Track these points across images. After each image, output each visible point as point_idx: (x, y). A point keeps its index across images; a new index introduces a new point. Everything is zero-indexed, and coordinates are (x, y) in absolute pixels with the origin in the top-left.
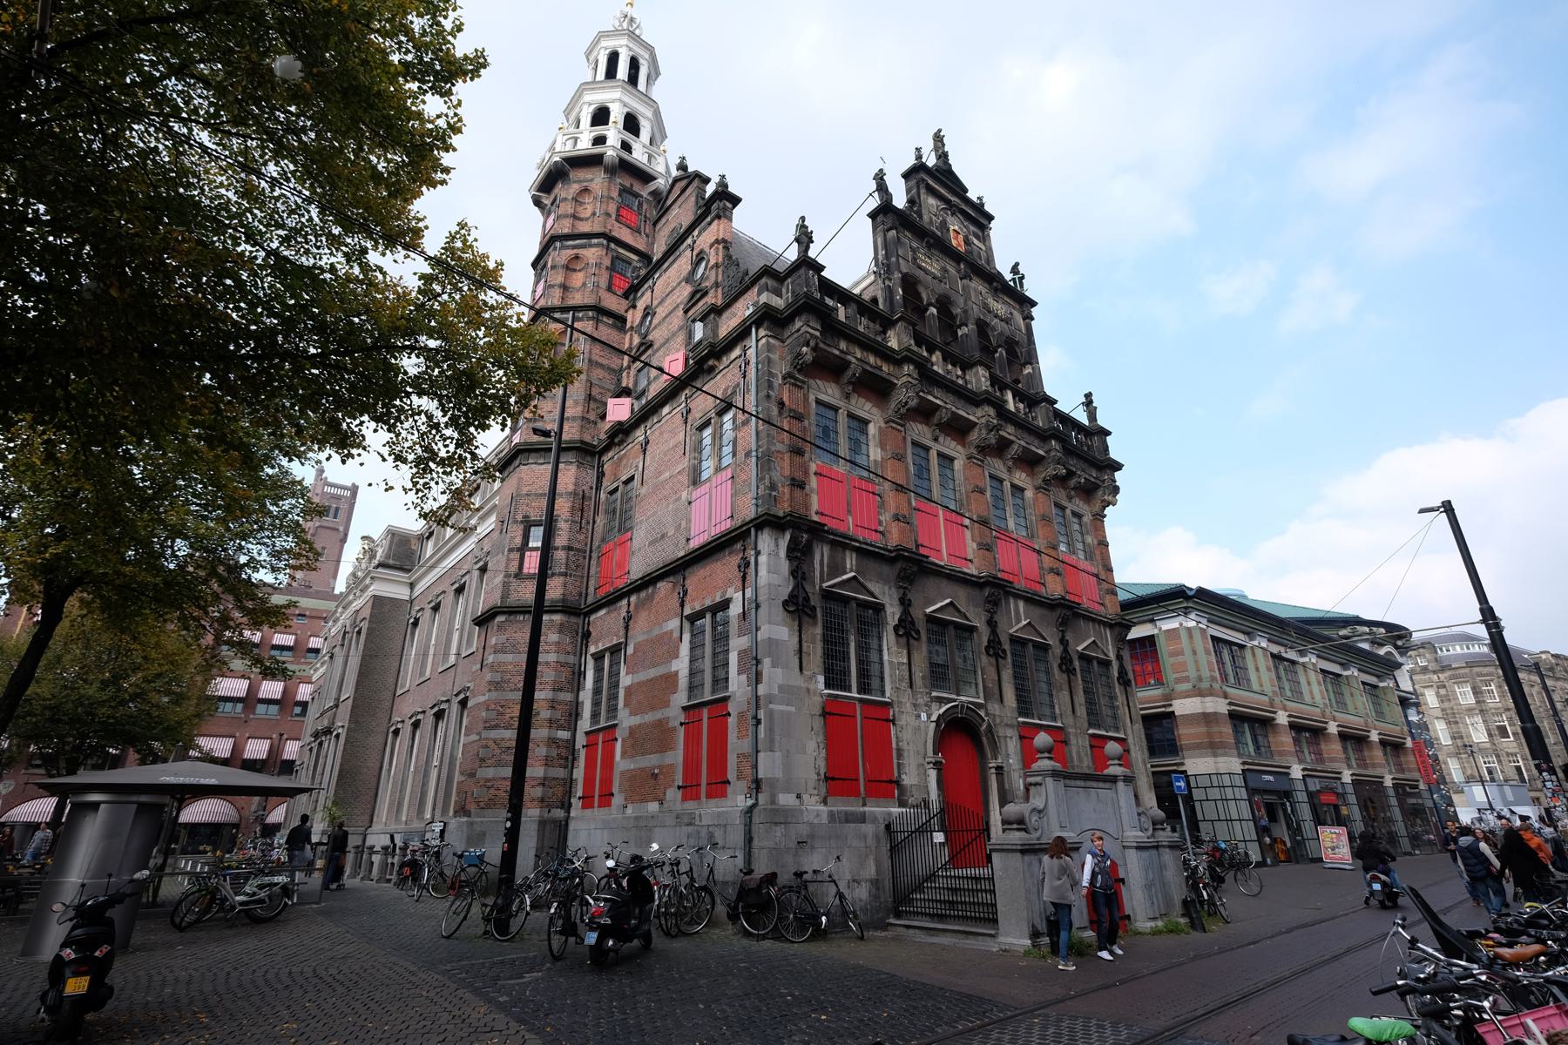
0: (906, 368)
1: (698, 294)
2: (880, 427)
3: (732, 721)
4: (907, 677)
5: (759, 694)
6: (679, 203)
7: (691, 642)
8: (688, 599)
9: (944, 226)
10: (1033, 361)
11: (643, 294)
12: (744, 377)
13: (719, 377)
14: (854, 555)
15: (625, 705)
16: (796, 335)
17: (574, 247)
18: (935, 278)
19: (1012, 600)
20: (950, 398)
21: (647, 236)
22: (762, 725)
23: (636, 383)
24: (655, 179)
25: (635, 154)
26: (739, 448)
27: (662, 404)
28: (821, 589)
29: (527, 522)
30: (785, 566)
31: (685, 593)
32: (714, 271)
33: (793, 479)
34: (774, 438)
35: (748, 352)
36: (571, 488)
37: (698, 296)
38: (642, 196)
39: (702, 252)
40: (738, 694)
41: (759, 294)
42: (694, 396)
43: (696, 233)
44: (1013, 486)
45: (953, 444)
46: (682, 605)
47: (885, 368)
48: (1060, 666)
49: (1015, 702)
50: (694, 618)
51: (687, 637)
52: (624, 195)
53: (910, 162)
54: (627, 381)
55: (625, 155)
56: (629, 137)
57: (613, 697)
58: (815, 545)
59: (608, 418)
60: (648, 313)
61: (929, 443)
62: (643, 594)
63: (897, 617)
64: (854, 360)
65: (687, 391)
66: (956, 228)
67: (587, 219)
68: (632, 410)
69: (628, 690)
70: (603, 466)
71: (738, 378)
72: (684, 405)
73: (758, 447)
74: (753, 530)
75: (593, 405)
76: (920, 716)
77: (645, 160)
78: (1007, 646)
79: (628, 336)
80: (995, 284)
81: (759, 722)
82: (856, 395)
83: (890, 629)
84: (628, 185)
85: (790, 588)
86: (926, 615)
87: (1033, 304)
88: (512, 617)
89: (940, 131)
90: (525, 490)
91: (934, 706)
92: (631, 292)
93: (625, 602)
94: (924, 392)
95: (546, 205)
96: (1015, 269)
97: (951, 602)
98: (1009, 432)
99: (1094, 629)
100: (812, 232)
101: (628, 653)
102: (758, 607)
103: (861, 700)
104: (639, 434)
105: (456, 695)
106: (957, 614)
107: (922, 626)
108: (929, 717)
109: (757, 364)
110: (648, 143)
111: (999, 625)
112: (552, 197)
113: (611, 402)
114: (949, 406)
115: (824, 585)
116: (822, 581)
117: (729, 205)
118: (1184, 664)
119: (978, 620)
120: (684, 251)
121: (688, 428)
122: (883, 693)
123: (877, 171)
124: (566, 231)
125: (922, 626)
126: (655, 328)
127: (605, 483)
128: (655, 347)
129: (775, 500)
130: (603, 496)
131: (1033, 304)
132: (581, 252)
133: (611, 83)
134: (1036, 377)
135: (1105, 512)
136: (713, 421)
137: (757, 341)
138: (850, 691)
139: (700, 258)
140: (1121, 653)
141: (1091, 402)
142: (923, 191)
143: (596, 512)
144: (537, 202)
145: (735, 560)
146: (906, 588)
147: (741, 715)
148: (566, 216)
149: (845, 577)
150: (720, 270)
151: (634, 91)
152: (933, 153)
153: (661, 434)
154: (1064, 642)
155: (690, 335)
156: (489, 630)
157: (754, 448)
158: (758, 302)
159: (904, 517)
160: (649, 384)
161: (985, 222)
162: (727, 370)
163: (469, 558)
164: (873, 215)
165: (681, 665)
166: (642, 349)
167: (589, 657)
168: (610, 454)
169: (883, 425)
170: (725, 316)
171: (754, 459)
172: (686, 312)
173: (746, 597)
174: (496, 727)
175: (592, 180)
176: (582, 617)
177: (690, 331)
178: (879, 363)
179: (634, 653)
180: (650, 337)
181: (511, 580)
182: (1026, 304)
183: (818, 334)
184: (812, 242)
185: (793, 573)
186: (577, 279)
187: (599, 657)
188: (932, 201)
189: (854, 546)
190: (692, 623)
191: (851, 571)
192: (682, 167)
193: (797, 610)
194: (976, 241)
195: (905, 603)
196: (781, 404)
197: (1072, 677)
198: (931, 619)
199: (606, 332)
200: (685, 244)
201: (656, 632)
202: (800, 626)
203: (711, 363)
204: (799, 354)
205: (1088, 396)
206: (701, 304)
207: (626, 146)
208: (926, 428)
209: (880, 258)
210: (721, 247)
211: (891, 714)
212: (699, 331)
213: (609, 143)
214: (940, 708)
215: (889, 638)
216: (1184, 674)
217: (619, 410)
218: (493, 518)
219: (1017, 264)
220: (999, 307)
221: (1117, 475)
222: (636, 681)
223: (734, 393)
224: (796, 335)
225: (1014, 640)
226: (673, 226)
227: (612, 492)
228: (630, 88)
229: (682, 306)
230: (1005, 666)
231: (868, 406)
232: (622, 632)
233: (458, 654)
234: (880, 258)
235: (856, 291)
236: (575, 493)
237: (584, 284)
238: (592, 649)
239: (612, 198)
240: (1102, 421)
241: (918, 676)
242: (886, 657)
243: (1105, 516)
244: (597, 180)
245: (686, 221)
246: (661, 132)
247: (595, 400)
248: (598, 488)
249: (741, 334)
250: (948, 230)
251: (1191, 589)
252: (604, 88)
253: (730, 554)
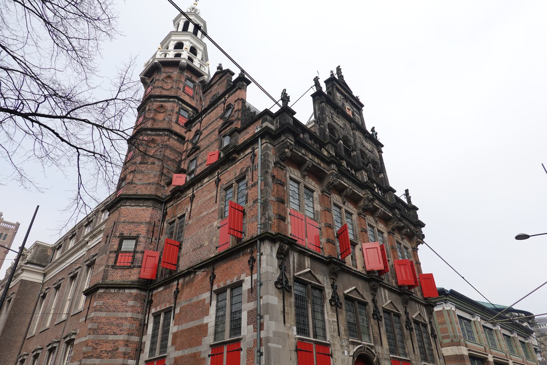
0: (332, 166)
1: (228, 123)
2: (319, 195)
3: (243, 354)
4: (337, 329)
5: (261, 337)
6: (218, 83)
7: (217, 306)
8: (216, 281)
9: (343, 104)
10: (384, 171)
11: (195, 125)
12: (253, 163)
13: (238, 163)
14: (309, 260)
15: (173, 344)
16: (282, 143)
17: (160, 101)
18: (341, 127)
19: (382, 289)
20: (350, 183)
21: (197, 101)
22: (264, 356)
23: (188, 167)
24: (203, 76)
25: (194, 63)
26: (249, 198)
27: (204, 178)
28: (294, 277)
29: (122, 237)
30: (276, 262)
31: (214, 277)
32: (237, 113)
33: (280, 216)
34: (270, 194)
35: (256, 151)
36: (148, 220)
37: (227, 124)
38: (196, 83)
39: (230, 104)
40: (247, 337)
41: (262, 123)
42: (223, 173)
43: (227, 96)
44: (379, 231)
45: (352, 207)
46: (212, 285)
47: (322, 165)
48: (406, 326)
49: (388, 346)
50: (220, 292)
51: (214, 303)
52: (187, 81)
53: (328, 76)
54: (184, 166)
55: (190, 63)
56: (192, 56)
57: (165, 339)
58: (290, 252)
59: (173, 184)
60: (198, 134)
61: (341, 205)
62: (187, 279)
63: (331, 295)
64: (308, 159)
65: (219, 170)
66: (349, 107)
67: (168, 90)
68: (186, 180)
69: (175, 335)
70: (166, 209)
71: (249, 163)
72: (216, 177)
73: (262, 197)
74: (258, 242)
75: (163, 177)
76: (344, 353)
77: (199, 66)
78: (382, 314)
79: (186, 144)
80: (366, 134)
81: (261, 354)
82: (308, 177)
83: (327, 301)
84: (190, 77)
85: (278, 275)
86: (344, 294)
87: (382, 146)
88: (108, 291)
89: (339, 66)
90: (122, 219)
91: (351, 346)
92: (188, 125)
93: (176, 283)
94: (340, 179)
95: (147, 83)
96: (373, 130)
97: (356, 289)
98: (377, 203)
99: (419, 307)
100: (289, 96)
101: (175, 313)
102: (261, 285)
103: (315, 342)
104: (189, 193)
105: (65, 338)
106: (358, 295)
107: (342, 300)
108: (349, 353)
109: (261, 156)
110: (200, 59)
111: (378, 302)
112: (151, 79)
113: (175, 175)
114: (351, 187)
115: (296, 274)
116: (294, 272)
117: (245, 84)
118: (446, 329)
119: (368, 299)
120: (220, 104)
121: (219, 189)
122: (325, 338)
123: (315, 77)
124: (157, 94)
125: (342, 300)
126: (202, 140)
127: (167, 218)
128: (201, 149)
129: (271, 226)
130: (165, 225)
131: (382, 146)
132: (164, 104)
133: (185, 33)
134: (385, 179)
135: (418, 247)
136: (234, 185)
137: (261, 145)
138: (309, 336)
139: (229, 107)
140: (431, 320)
141: (408, 194)
142: (335, 89)
143: (161, 233)
144: (143, 81)
145: (246, 258)
146: (334, 279)
147: (249, 350)
148: (158, 87)
149: (305, 271)
150: (240, 113)
151: (195, 37)
153: (203, 192)
154: (406, 313)
155: (221, 143)
156: (93, 298)
157: (259, 198)
158: (262, 126)
159: (332, 241)
160: (197, 167)
161: (360, 107)
162: (243, 159)
163: (81, 259)
164: (313, 96)
165: (210, 320)
166: (194, 150)
167: (151, 315)
168: (171, 203)
169: (320, 193)
170: (242, 134)
171: (259, 204)
172: (220, 132)
173: (253, 279)
174: (91, 357)
175: (172, 72)
176: (148, 291)
177: (222, 141)
178: (319, 162)
179: (180, 312)
180: (198, 145)
181: (110, 268)
182: (379, 145)
183: (293, 143)
184: (289, 101)
185: (280, 266)
186: (160, 117)
187: (157, 316)
188: (338, 94)
189: (309, 254)
190: (218, 295)
191: (308, 268)
192: (220, 67)
193: (282, 288)
194: (356, 115)
195: (333, 287)
196: (273, 177)
197: (412, 333)
199: (173, 142)
200: (220, 101)
201: (195, 300)
202: (283, 297)
203: (234, 156)
204: (284, 152)
205: (407, 191)
206: (228, 128)
207: (190, 59)
208: (339, 198)
209: (317, 115)
210: (241, 102)
211: (330, 351)
212: (226, 142)
213: (182, 57)
214: (354, 348)
215: (327, 307)
216: (447, 334)
217: (179, 180)
218: (101, 235)
219: (374, 128)
220: (368, 145)
221: (423, 229)
222: (180, 329)
223: (247, 170)
224: (282, 143)
225: (386, 311)
226: (214, 93)
227: (171, 223)
228: (193, 36)
229: (218, 130)
230: (382, 325)
231: (313, 183)
232: (173, 301)
233: (68, 314)
234: (317, 115)
235: (309, 127)
236: (149, 223)
237: (164, 119)
238: (153, 310)
239: (182, 81)
240: (414, 203)
241: (342, 329)
242: (326, 317)
243: (418, 249)
244: (175, 73)
245: (221, 91)
246: (206, 57)
247: (165, 175)
248: (163, 221)
249: (252, 141)
250: (345, 108)
251: (447, 291)
252: (182, 35)
253: (243, 255)
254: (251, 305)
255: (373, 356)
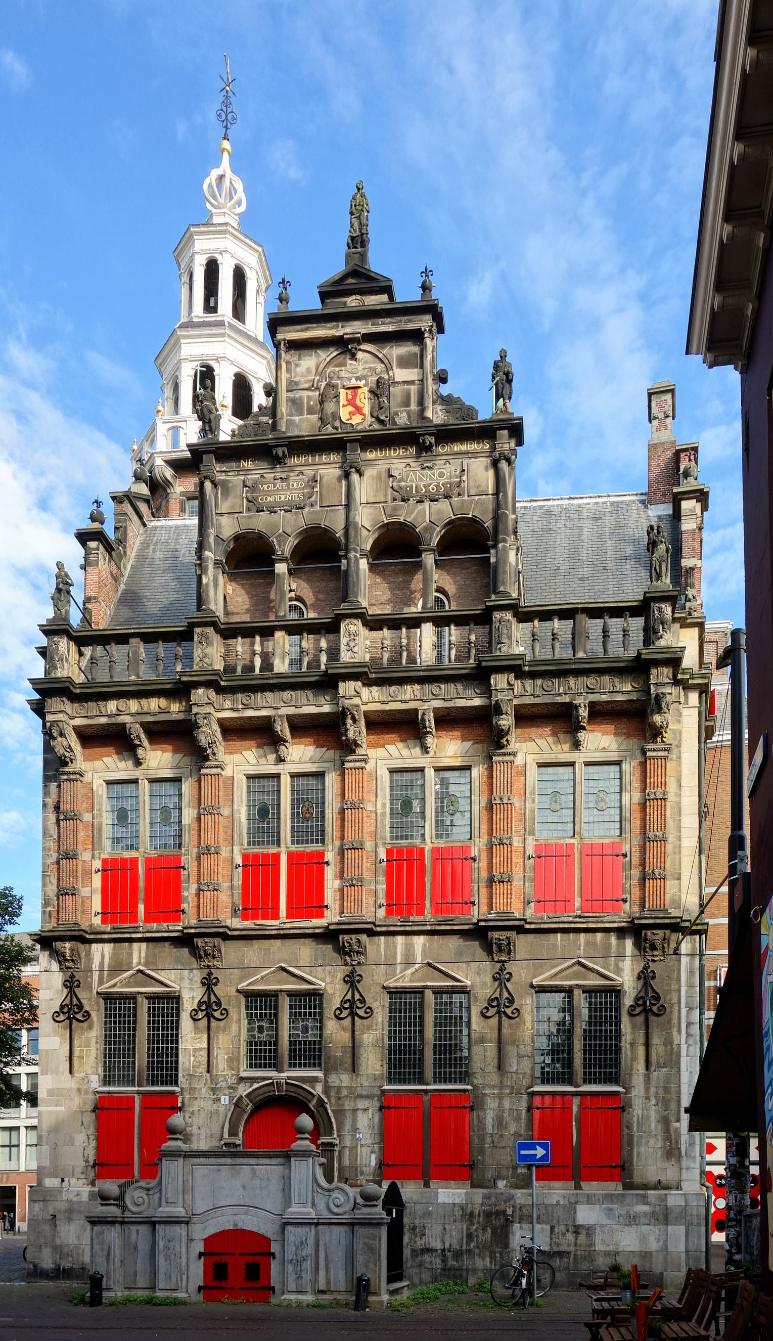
4: (205, 1062)
76: (219, 1099)
106: (293, 979)
146: (209, 966)
178: (163, 702)
255: (309, 1097)
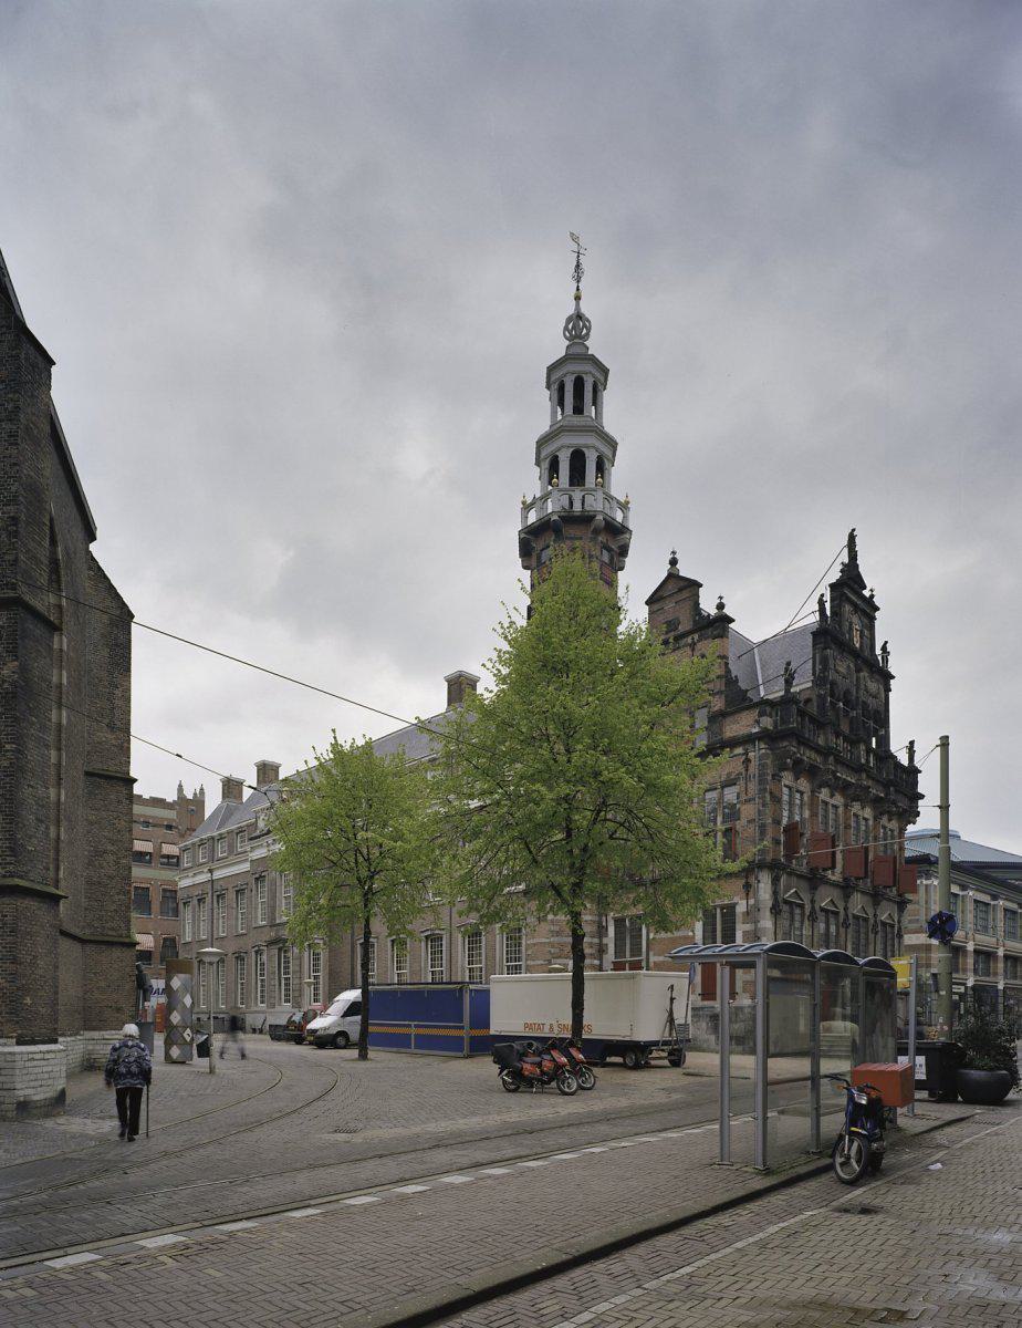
152: (846, 550)
182: (886, 677)
198: (822, 910)
204: (786, 763)
225: (856, 917)
254: (748, 927)
